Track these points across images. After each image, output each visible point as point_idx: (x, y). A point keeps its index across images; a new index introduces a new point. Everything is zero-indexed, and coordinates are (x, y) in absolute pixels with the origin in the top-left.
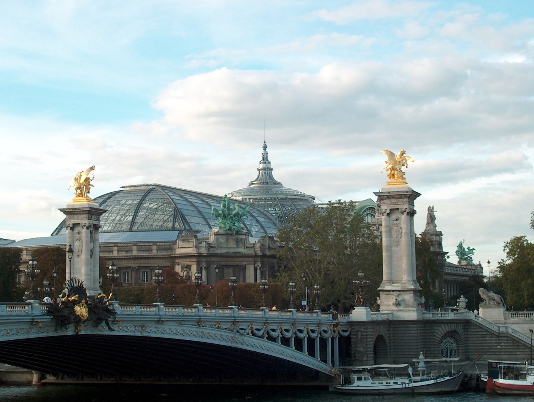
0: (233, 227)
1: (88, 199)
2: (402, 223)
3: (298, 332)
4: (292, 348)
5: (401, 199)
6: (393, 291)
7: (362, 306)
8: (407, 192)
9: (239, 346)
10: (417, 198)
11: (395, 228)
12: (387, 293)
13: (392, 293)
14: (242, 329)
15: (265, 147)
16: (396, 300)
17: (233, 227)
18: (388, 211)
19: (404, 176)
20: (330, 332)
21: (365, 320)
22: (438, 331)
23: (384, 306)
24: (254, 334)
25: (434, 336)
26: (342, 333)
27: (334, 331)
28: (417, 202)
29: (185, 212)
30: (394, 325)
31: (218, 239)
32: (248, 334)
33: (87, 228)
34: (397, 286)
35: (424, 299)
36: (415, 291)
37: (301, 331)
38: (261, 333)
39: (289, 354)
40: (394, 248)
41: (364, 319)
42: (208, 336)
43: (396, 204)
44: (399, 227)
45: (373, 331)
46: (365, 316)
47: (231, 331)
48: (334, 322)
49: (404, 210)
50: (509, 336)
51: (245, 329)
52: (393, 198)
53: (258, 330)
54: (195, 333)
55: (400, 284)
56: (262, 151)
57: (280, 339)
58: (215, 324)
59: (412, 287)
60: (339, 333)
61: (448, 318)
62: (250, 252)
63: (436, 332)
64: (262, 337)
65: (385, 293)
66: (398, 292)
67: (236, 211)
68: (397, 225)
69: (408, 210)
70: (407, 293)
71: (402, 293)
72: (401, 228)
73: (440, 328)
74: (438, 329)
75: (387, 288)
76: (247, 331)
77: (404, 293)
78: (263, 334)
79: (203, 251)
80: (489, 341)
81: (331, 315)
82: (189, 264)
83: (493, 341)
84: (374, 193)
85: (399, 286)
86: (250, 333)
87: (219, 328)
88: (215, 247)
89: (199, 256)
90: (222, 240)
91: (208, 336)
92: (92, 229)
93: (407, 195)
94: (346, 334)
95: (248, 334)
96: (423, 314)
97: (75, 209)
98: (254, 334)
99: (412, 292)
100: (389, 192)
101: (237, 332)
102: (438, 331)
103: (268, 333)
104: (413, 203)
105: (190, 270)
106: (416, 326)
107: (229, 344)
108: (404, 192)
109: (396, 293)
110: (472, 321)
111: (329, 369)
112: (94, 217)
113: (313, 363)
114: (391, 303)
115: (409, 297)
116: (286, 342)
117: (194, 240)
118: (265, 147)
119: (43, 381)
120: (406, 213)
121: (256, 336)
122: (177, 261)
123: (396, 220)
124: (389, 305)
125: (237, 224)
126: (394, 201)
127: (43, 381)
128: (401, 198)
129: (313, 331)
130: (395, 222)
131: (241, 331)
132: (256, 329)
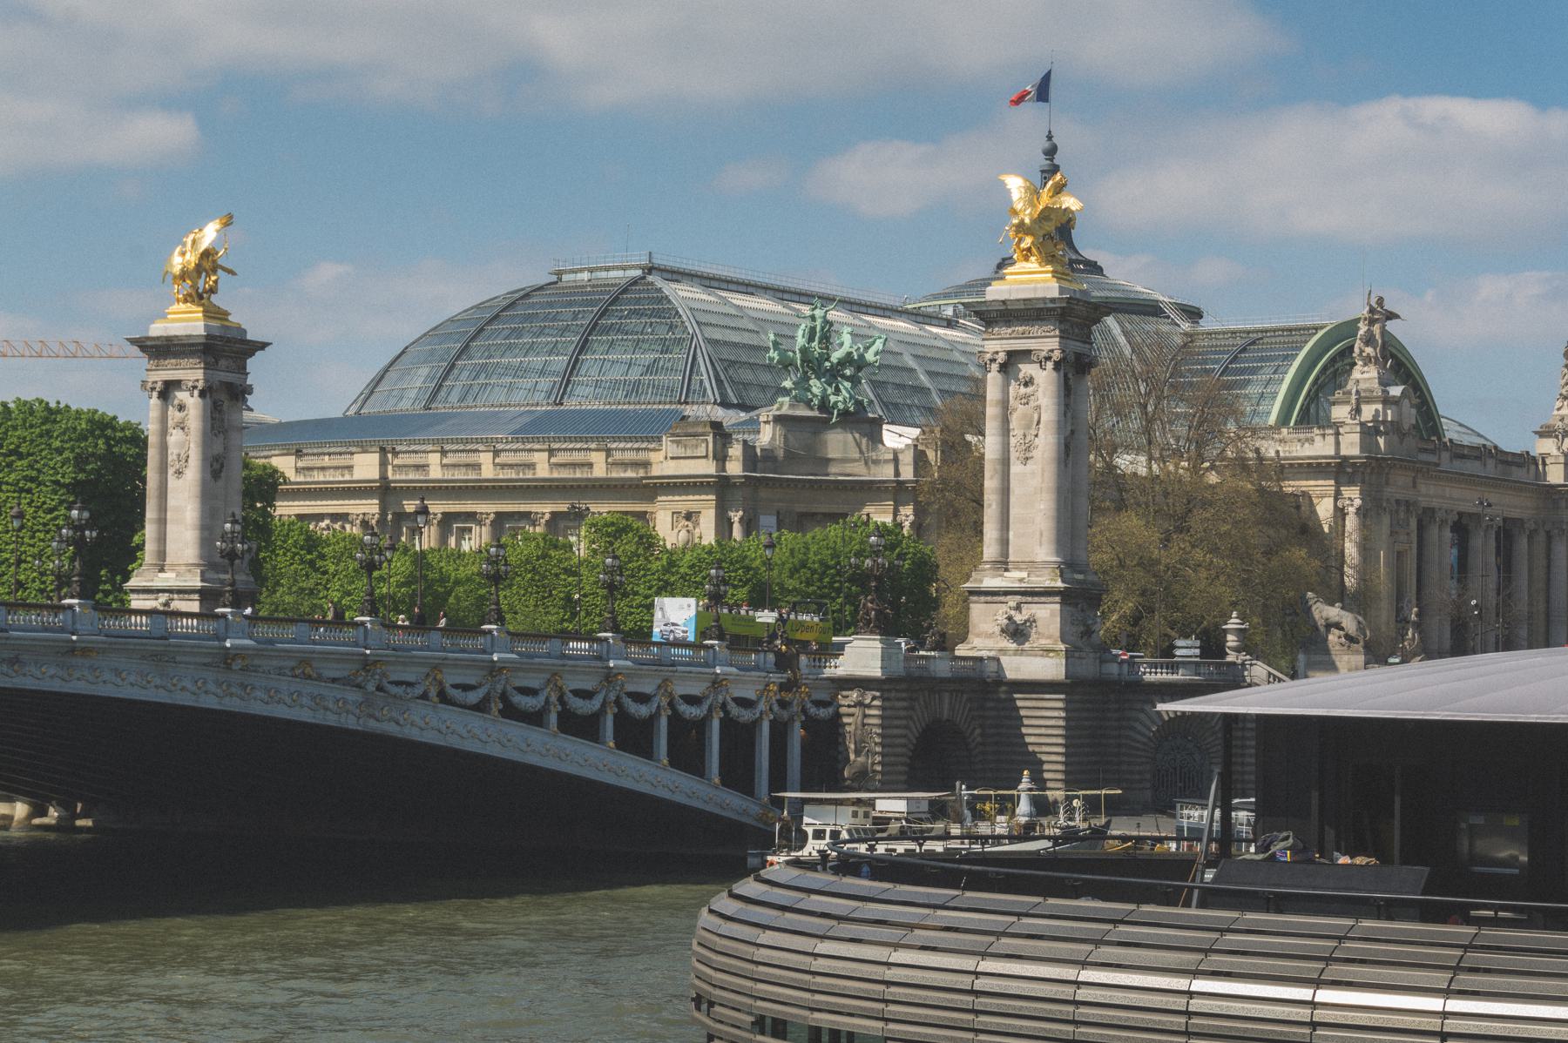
0: (833, 399)
1: (212, 313)
2: (1040, 394)
3: (627, 702)
4: (604, 743)
6: (1006, 593)
7: (872, 632)
8: (1053, 300)
9: (391, 729)
12: (989, 598)
13: (1002, 599)
14: (398, 683)
16: (1010, 618)
18: (1001, 357)
20: (762, 706)
21: (876, 672)
22: (1142, 716)
23: (978, 635)
24: (444, 698)
25: (1132, 728)
26: (813, 710)
27: (783, 704)
30: (990, 692)
32: (424, 696)
33: (202, 394)
37: (642, 698)
38: (473, 697)
39: (599, 762)
40: (1016, 468)
41: (874, 670)
42: (266, 698)
44: (1032, 404)
45: (913, 708)
47: (359, 686)
48: (777, 678)
49: (1044, 354)
51: (409, 684)
53: (466, 688)
54: (211, 687)
55: (1024, 574)
57: (553, 718)
58: (293, 664)
59: (1059, 584)
60: (804, 711)
62: (886, 473)
63: (1137, 720)
64: (481, 707)
65: (983, 599)
66: (1018, 598)
67: (846, 348)
68: (1026, 400)
72: (1038, 407)
74: (1143, 711)
75: (990, 582)
76: (419, 691)
78: (486, 699)
79: (734, 468)
81: (771, 657)
82: (693, 507)
85: (1021, 580)
86: (433, 692)
87: (310, 677)
89: (722, 487)
91: (266, 698)
92: (223, 397)
93: (1054, 309)
94: (823, 713)
95: (424, 696)
97: (168, 339)
98: (444, 698)
99: (1058, 599)
100: (1004, 302)
101: (380, 688)
102: (1142, 716)
103: (504, 697)
105: (696, 524)
107: (351, 723)
108: (1044, 299)
109: (1012, 601)
111: (755, 809)
112: (223, 363)
113: (701, 792)
114: (997, 630)
115: (1048, 615)
116: (581, 727)
117: (710, 439)
119: (37, 821)
120: (1050, 365)
121: (454, 704)
123: (1026, 385)
124: (990, 636)
127: (37, 821)
129: (692, 700)
130: (1023, 390)
131: (394, 690)
132: (455, 686)
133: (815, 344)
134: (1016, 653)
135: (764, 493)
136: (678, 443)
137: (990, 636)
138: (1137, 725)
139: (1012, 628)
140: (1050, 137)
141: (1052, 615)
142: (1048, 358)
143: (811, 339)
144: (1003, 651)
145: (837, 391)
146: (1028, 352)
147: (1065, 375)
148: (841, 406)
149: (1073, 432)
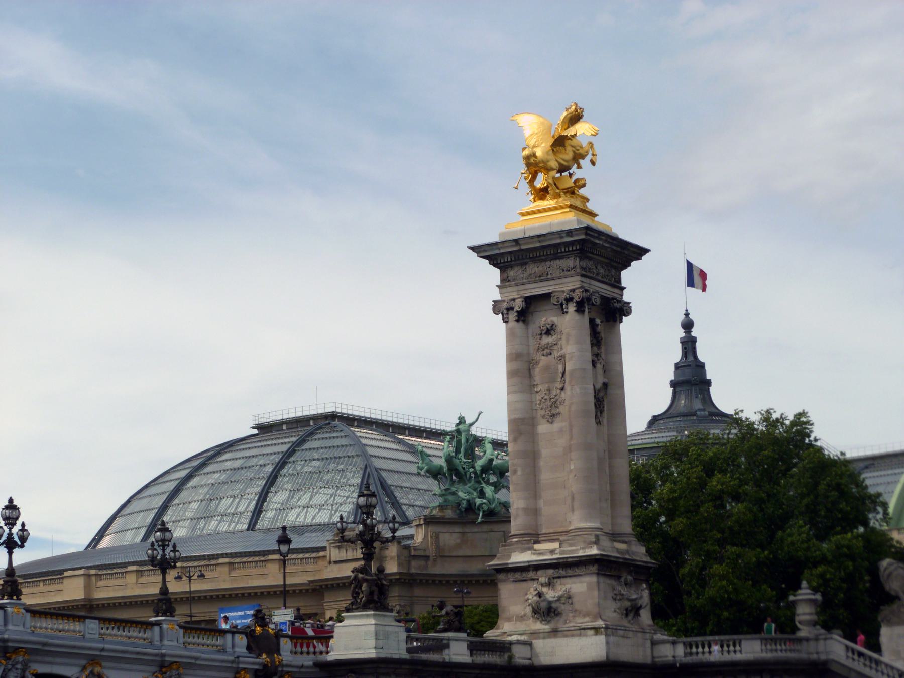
0: (478, 501)
5: (558, 262)
7: (365, 607)
8: (569, 232)
11: (544, 361)
12: (518, 575)
13: (531, 574)
15: (688, 325)
16: (540, 595)
17: (478, 501)
18: (518, 305)
19: (582, 191)
23: (509, 619)
28: (627, 276)
29: (391, 480)
31: (436, 537)
34: (547, 551)
35: (646, 594)
36: (604, 566)
43: (542, 278)
46: (372, 643)
49: (563, 297)
55: (555, 545)
56: (681, 333)
59: (594, 551)
61: (738, 657)
65: (511, 576)
66: (550, 572)
69: (577, 296)
70: (578, 571)
71: (562, 572)
75: (519, 558)
77: (570, 572)
84: (473, 249)
85: (552, 552)
88: (427, 558)
90: (449, 538)
93: (572, 243)
96: (654, 643)
99: (594, 568)
104: (619, 281)
110: (834, 668)
114: (529, 610)
118: (688, 325)
120: (572, 308)
122: (328, 597)
123: (548, 332)
125: (489, 490)
126: (534, 268)
128: (556, 257)
130: (546, 340)
133: (461, 456)
134: (555, 632)
135: (418, 591)
136: (339, 548)
137: (522, 618)
139: (544, 605)
140: (687, 315)
141: (589, 588)
142: (569, 300)
143: (457, 451)
144: (535, 634)
145: (482, 494)
146: (547, 297)
147: (592, 321)
148: (485, 507)
149: (605, 385)
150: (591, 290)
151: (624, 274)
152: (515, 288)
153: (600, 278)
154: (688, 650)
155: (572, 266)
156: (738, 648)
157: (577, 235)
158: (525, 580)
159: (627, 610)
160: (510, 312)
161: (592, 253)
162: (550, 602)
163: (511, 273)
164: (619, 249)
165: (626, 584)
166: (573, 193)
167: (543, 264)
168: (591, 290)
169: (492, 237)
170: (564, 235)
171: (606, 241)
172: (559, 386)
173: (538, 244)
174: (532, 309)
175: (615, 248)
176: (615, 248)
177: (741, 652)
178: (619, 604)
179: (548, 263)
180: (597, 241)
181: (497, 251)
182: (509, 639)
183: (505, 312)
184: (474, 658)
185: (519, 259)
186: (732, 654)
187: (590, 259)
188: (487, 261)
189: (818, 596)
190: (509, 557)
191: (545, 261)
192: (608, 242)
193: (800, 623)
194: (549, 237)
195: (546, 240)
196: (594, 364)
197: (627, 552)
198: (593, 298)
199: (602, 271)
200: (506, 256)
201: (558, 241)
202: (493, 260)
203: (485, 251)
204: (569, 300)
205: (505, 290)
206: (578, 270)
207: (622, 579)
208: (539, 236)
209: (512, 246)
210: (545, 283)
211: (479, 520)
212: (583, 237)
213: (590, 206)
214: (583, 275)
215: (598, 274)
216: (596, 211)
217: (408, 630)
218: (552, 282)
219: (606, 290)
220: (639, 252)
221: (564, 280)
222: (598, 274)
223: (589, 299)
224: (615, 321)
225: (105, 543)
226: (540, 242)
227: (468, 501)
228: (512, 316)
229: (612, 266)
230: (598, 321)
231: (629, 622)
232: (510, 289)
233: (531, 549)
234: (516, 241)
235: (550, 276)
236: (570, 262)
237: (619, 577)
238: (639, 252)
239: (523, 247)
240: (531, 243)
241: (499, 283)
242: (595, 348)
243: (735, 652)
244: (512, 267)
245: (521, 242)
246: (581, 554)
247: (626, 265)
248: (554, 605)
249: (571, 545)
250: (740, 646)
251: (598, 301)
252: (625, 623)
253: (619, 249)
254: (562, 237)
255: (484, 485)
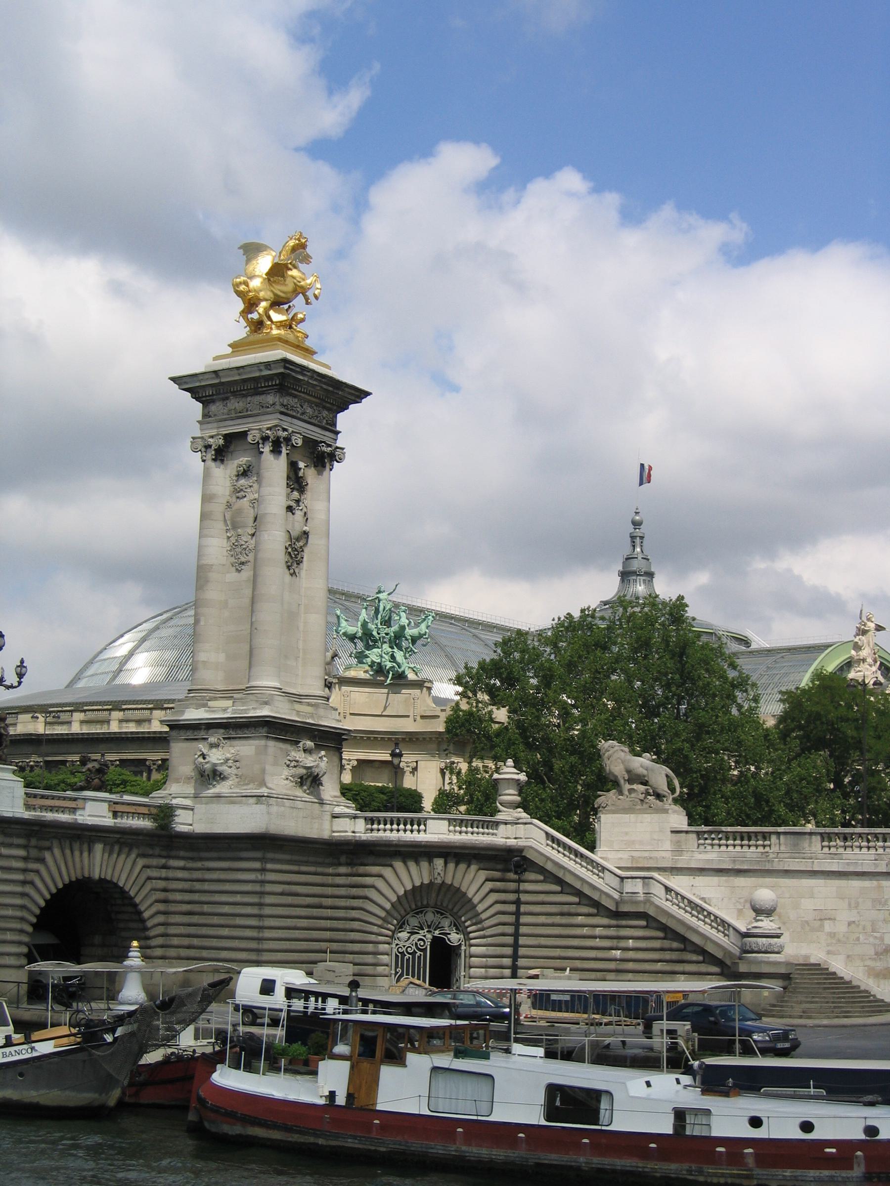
10: (351, 406)
12: (190, 734)
13: (202, 734)
19: (300, 327)
22: (379, 883)
23: (177, 781)
28: (343, 420)
43: (242, 415)
50: (651, 912)
52: (235, 394)
61: (421, 837)
65: (184, 734)
73: (387, 872)
80: (585, 931)
83: (598, 931)
85: (225, 710)
99: (263, 731)
104: (335, 425)
106: (258, 854)
126: (235, 404)
128: (257, 392)
138: (372, 894)
147: (293, 466)
150: (290, 430)
151: (341, 417)
152: (215, 425)
153: (306, 418)
154: (369, 826)
155: (271, 402)
156: (422, 827)
157: (276, 368)
158: (196, 739)
159: (301, 778)
160: (209, 450)
161: (297, 390)
162: (215, 765)
163: (213, 408)
164: (331, 389)
165: (305, 751)
166: (291, 327)
167: (244, 399)
168: (290, 430)
169: (198, 367)
170: (262, 368)
171: (311, 378)
172: (251, 531)
173: (237, 378)
174: (232, 448)
175: (324, 386)
176: (324, 386)
177: (425, 831)
178: (293, 771)
179: (249, 399)
180: (301, 377)
181: (197, 384)
182: (174, 802)
183: (203, 449)
184: (119, 820)
185: (220, 394)
186: (401, 833)
187: (295, 396)
188: (189, 394)
189: (523, 777)
190: (183, 713)
191: (245, 396)
192: (316, 380)
193: (501, 804)
194: (248, 369)
195: (245, 373)
196: (290, 509)
197: (312, 716)
198: (293, 438)
199: (309, 410)
200: (208, 389)
201: (257, 374)
202: (195, 393)
203: (186, 383)
204: (265, 439)
205: (205, 426)
206: (278, 407)
207: (301, 744)
208: (238, 368)
209: (212, 378)
210: (239, 421)
211: (388, 682)
212: (282, 370)
213: (308, 343)
214: (282, 413)
215: (303, 414)
216: (315, 349)
217: (27, 786)
218: (251, 420)
219: (316, 433)
220: (359, 395)
221: (263, 418)
222: (303, 414)
223: (288, 440)
224: (324, 466)
225: (81, 684)
226: (239, 375)
227: (379, 664)
228: (211, 453)
229: (324, 408)
230: (301, 465)
231: (305, 791)
232: (210, 426)
233: (205, 706)
234: (216, 373)
235: (249, 413)
236: (270, 399)
237: (298, 742)
238: (359, 395)
239: (223, 380)
240: (229, 376)
241: (200, 419)
242: (296, 494)
243: (419, 831)
244: (213, 401)
245: (221, 374)
246: (251, 714)
247: (344, 407)
248: (219, 768)
249: (243, 704)
250: (425, 825)
251: (300, 442)
252: (299, 792)
253: (331, 389)
254: (261, 370)
255: (396, 650)
